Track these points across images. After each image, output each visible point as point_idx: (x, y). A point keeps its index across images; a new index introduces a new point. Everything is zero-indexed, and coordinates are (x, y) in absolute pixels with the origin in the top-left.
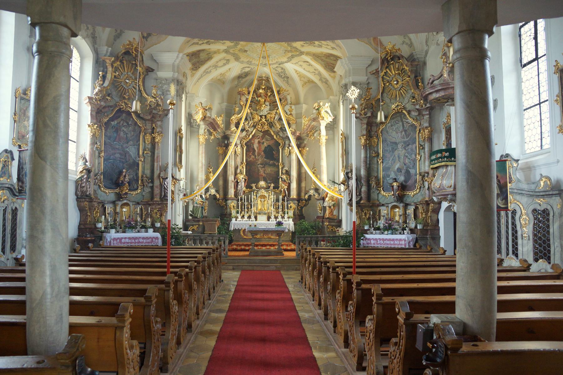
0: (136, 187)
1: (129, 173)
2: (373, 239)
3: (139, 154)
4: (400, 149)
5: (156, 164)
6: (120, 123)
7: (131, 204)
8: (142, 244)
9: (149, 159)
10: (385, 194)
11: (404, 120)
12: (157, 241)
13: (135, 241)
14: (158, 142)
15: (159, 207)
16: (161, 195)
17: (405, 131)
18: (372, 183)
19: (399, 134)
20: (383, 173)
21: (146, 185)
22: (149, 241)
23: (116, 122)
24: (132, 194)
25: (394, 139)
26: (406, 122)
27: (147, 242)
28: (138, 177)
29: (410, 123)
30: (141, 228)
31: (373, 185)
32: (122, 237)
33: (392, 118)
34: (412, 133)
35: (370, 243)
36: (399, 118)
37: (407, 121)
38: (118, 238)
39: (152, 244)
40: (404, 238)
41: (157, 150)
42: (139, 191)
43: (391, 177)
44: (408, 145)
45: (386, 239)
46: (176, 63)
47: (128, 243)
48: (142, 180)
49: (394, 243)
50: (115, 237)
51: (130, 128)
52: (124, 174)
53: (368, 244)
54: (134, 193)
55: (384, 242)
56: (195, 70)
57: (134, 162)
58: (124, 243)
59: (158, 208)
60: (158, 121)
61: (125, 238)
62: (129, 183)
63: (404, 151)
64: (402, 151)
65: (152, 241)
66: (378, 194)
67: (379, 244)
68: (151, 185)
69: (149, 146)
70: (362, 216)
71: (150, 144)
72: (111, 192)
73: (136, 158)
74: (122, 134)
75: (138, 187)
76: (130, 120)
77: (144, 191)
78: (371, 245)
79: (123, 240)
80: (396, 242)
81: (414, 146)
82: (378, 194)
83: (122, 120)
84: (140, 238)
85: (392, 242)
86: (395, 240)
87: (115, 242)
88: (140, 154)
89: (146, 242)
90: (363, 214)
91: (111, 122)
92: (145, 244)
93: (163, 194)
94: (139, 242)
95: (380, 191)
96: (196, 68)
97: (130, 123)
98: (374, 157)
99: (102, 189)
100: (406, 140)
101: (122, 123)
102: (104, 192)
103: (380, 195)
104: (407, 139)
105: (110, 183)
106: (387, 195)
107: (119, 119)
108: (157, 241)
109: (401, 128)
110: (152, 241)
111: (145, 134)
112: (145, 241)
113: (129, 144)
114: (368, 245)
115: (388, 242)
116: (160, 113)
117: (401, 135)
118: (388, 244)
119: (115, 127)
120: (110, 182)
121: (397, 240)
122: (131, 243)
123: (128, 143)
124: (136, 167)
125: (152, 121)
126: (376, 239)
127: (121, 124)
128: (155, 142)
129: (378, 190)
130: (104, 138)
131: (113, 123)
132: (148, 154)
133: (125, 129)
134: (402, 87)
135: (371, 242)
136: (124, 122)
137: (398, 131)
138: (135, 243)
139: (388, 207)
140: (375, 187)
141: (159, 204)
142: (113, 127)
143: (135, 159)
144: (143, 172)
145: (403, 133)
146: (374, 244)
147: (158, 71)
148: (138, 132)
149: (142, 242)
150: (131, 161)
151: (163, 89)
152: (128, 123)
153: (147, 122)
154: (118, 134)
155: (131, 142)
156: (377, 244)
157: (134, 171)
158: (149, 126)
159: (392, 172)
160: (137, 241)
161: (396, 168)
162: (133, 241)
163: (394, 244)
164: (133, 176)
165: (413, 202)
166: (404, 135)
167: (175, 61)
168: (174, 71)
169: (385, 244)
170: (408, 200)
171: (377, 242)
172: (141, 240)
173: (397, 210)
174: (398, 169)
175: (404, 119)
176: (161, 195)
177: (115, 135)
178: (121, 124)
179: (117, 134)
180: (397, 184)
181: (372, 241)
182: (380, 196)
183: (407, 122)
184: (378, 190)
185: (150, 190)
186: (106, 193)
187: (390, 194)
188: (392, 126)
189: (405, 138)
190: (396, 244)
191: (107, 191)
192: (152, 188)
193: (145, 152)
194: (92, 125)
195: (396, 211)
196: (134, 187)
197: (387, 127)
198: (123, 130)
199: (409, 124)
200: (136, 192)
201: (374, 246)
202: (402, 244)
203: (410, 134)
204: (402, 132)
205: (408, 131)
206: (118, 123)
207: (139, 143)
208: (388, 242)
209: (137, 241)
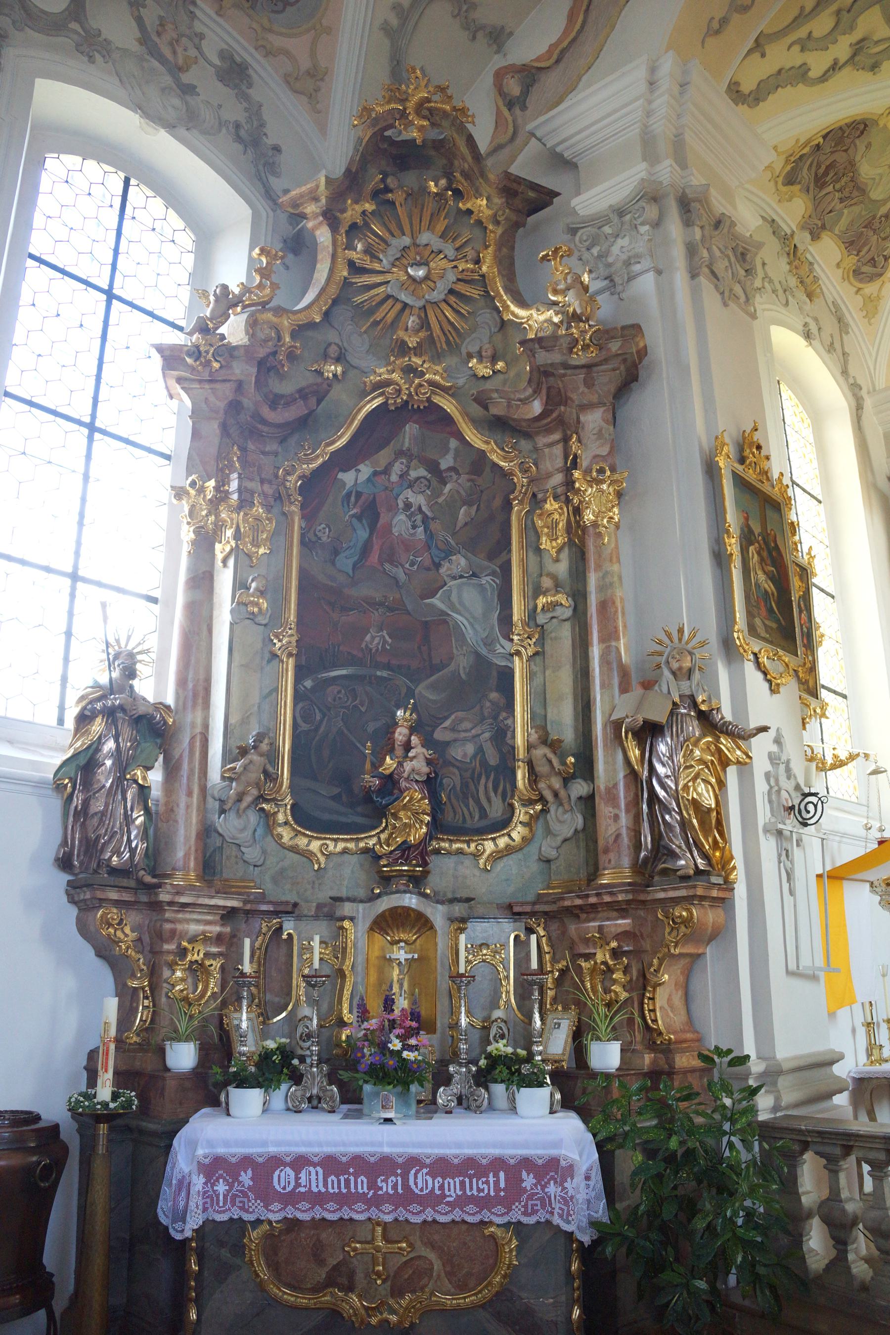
0: (496, 810)
1: (453, 729)
3: (506, 621)
5: (595, 651)
6: (386, 471)
7: (437, 915)
8: (429, 1215)
9: (566, 633)
12: (552, 1189)
13: (372, 1185)
14: (595, 524)
15: (624, 923)
16: (637, 846)
21: (556, 795)
22: (487, 1186)
23: (365, 470)
24: (476, 856)
27: (472, 1200)
28: (508, 754)
30: (483, 1079)
32: (272, 1149)
38: (247, 1161)
39: (516, 1215)
41: (598, 567)
42: (518, 833)
46: (660, 126)
47: (318, 1199)
48: (530, 764)
50: (221, 1151)
51: (448, 487)
52: (401, 734)
54: (489, 846)
56: (872, 278)
57: (481, 663)
58: (291, 1198)
59: (617, 937)
60: (584, 407)
61: (300, 1163)
62: (431, 784)
65: (514, 1190)
68: (580, 788)
69: (562, 568)
71: (565, 555)
72: (341, 846)
73: (489, 643)
74: (400, 524)
75: (512, 807)
76: (445, 450)
77: (548, 832)
79: (283, 1179)
83: (400, 454)
84: (414, 1162)
87: (221, 1188)
88: (515, 618)
89: (462, 1201)
91: (341, 476)
92: (457, 1215)
93: (647, 839)
94: (407, 1198)
96: (873, 262)
97: (444, 466)
99: (286, 835)
101: (397, 468)
102: (295, 849)
105: (336, 798)
107: (384, 456)
108: (552, 1189)
110: (514, 1190)
111: (536, 502)
112: (453, 1188)
113: (442, 570)
116: (579, 358)
119: (359, 495)
120: (336, 791)
122: (345, 1199)
123: (438, 566)
124: (494, 695)
125: (561, 422)
127: (394, 478)
128: (584, 529)
130: (302, 556)
131: (348, 478)
132: (559, 611)
133: (417, 499)
136: (415, 462)
138: (376, 1201)
141: (621, 910)
142: (349, 495)
143: (484, 651)
144: (540, 722)
147: (578, 193)
148: (498, 502)
149: (433, 1200)
150: (462, 663)
151: (610, 260)
152: (433, 467)
153: (542, 441)
154: (382, 521)
155: (460, 562)
157: (483, 719)
158: (554, 459)
160: (386, 1186)
162: (362, 1185)
164: (480, 750)
167: (649, 114)
168: (650, 153)
172: (422, 1182)
176: (637, 846)
177: (363, 534)
178: (394, 478)
179: (373, 527)
185: (579, 821)
186: (308, 855)
191: (315, 846)
192: (589, 802)
193: (542, 601)
194: (193, 484)
196: (483, 814)
198: (408, 506)
200: (502, 842)
206: (375, 474)
207: (509, 562)
209: (386, 1186)
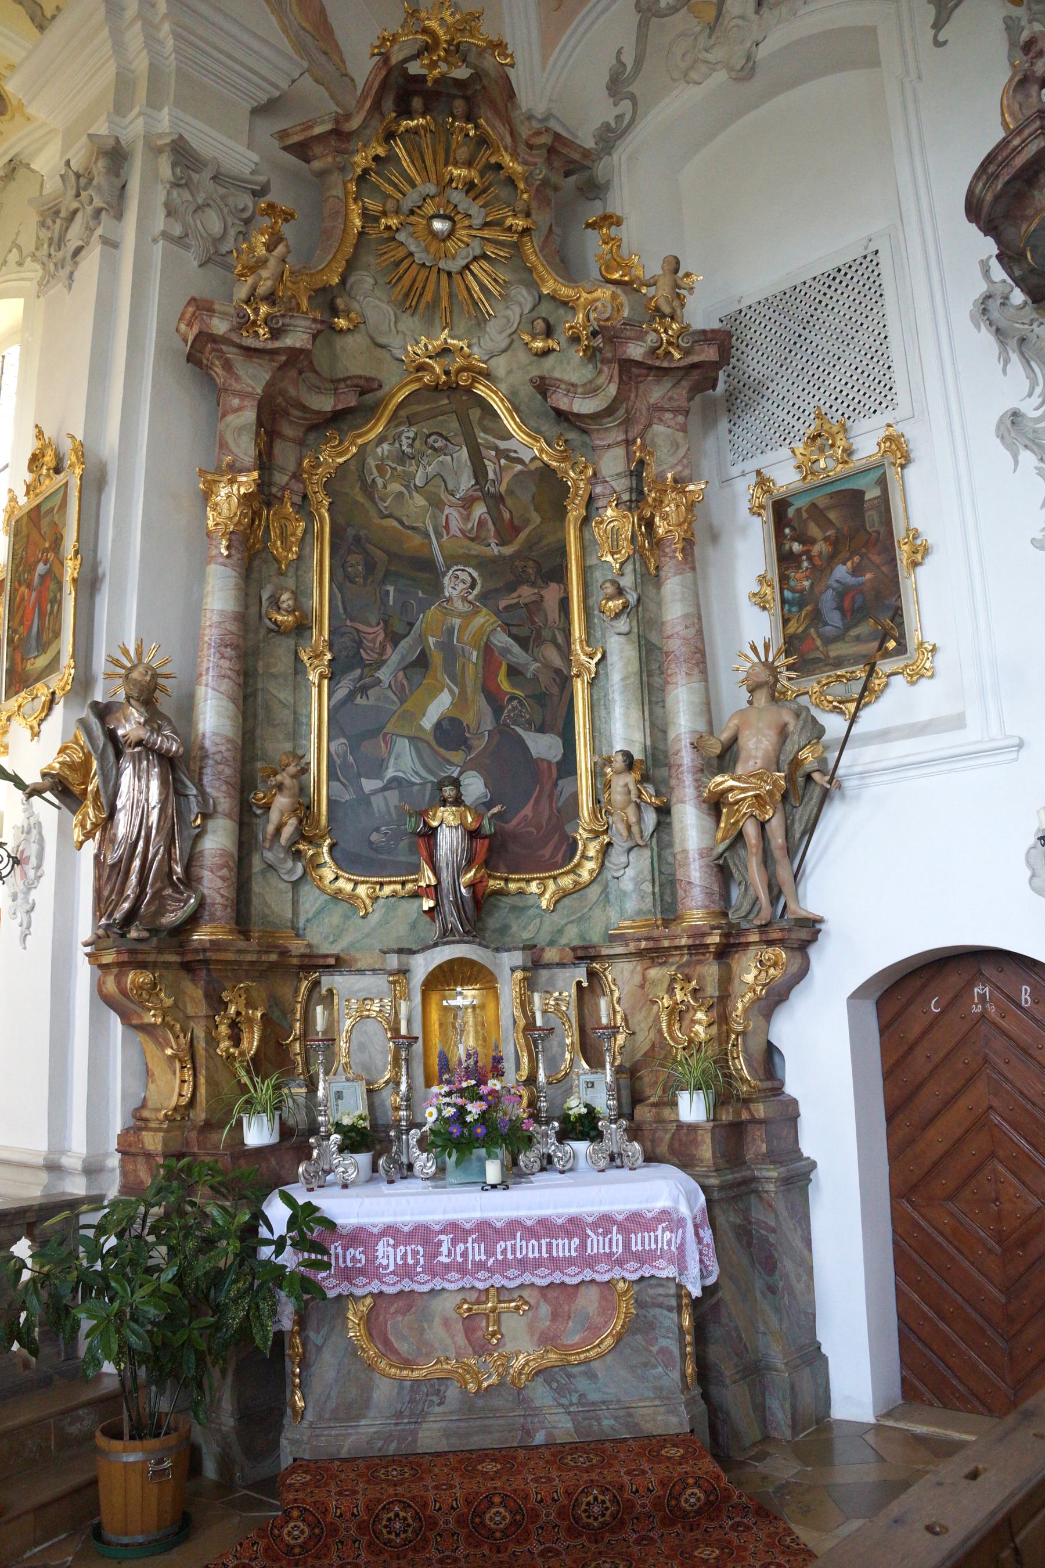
2: (390, 1230)
4: (460, 606)
10: (348, 887)
11: (482, 437)
17: (495, 501)
18: (267, 808)
19: (453, 514)
20: (334, 745)
25: (417, 540)
26: (496, 449)
29: (520, 461)
31: (274, 816)
33: (403, 413)
34: (536, 519)
35: (371, 1270)
36: (454, 424)
37: (503, 445)
40: (663, 1203)
43: (390, 773)
44: (511, 587)
45: (513, 1227)
49: (581, 1247)
53: (348, 1274)
55: (490, 1252)
63: (483, 619)
64: (468, 617)
66: (296, 884)
67: (454, 1266)
70: (212, 1041)
78: (375, 1287)
80: (596, 1244)
81: (551, 594)
82: (296, 884)
85: (565, 1247)
86: (594, 1227)
90: (224, 1030)
95: (315, 864)
98: (278, 630)
100: (495, 550)
103: (306, 889)
104: (508, 550)
106: (362, 890)
109: (466, 482)
114: (345, 1289)
115: (532, 1249)
117: (467, 518)
118: (526, 1265)
121: (605, 1222)
126: (423, 1235)
129: (298, 855)
134: (475, 259)
135: (372, 1257)
137: (444, 496)
139: (404, 972)
140: (287, 832)
145: (480, 510)
146: (405, 1271)
156: (435, 1270)
159: (403, 745)
161: (428, 722)
163: (583, 1261)
165: (552, 943)
166: (481, 523)
169: (500, 1268)
170: (514, 929)
171: (433, 1249)
173: (466, 997)
174: (438, 726)
175: (485, 430)
180: (463, 818)
181: (380, 1249)
182: (311, 900)
183: (501, 453)
184: (298, 855)
187: (388, 890)
188: (403, 458)
189: (493, 541)
190: (599, 1258)
195: (459, 1001)
197: (372, 462)
199: (519, 467)
201: (407, 1285)
202: (648, 1257)
203: (527, 522)
204: (467, 503)
205: (509, 501)
208: (532, 1249)
